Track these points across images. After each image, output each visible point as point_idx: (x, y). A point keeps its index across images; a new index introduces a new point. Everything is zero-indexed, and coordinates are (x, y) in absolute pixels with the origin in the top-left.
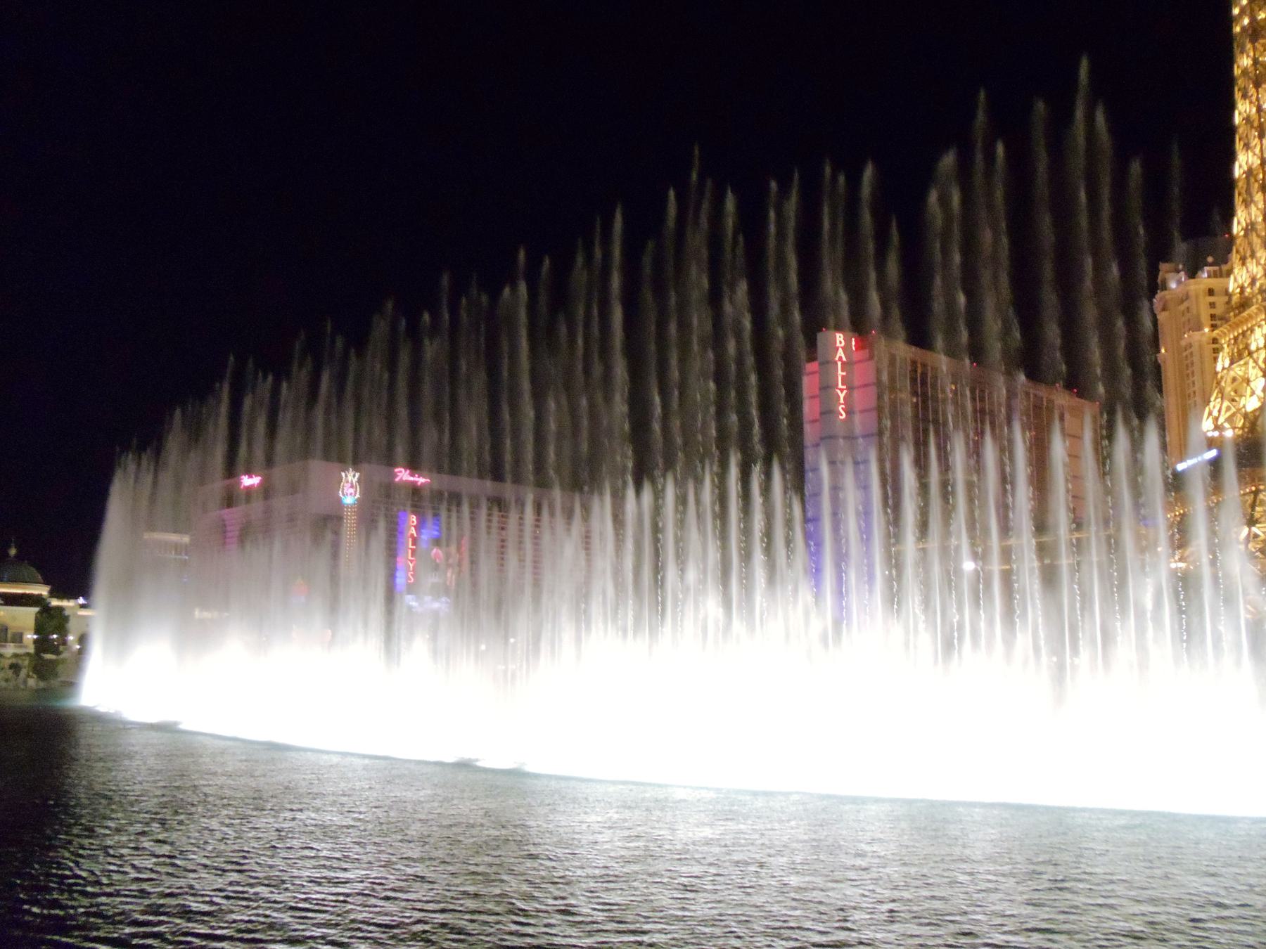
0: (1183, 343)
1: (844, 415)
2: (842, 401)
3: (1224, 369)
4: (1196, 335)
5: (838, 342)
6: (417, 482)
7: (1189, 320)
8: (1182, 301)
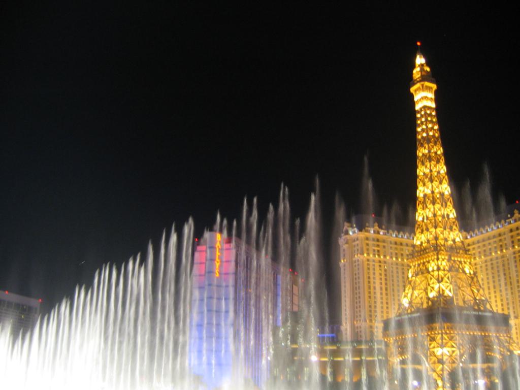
0: (354, 259)
1: (217, 275)
2: (217, 267)
8: (354, 241)
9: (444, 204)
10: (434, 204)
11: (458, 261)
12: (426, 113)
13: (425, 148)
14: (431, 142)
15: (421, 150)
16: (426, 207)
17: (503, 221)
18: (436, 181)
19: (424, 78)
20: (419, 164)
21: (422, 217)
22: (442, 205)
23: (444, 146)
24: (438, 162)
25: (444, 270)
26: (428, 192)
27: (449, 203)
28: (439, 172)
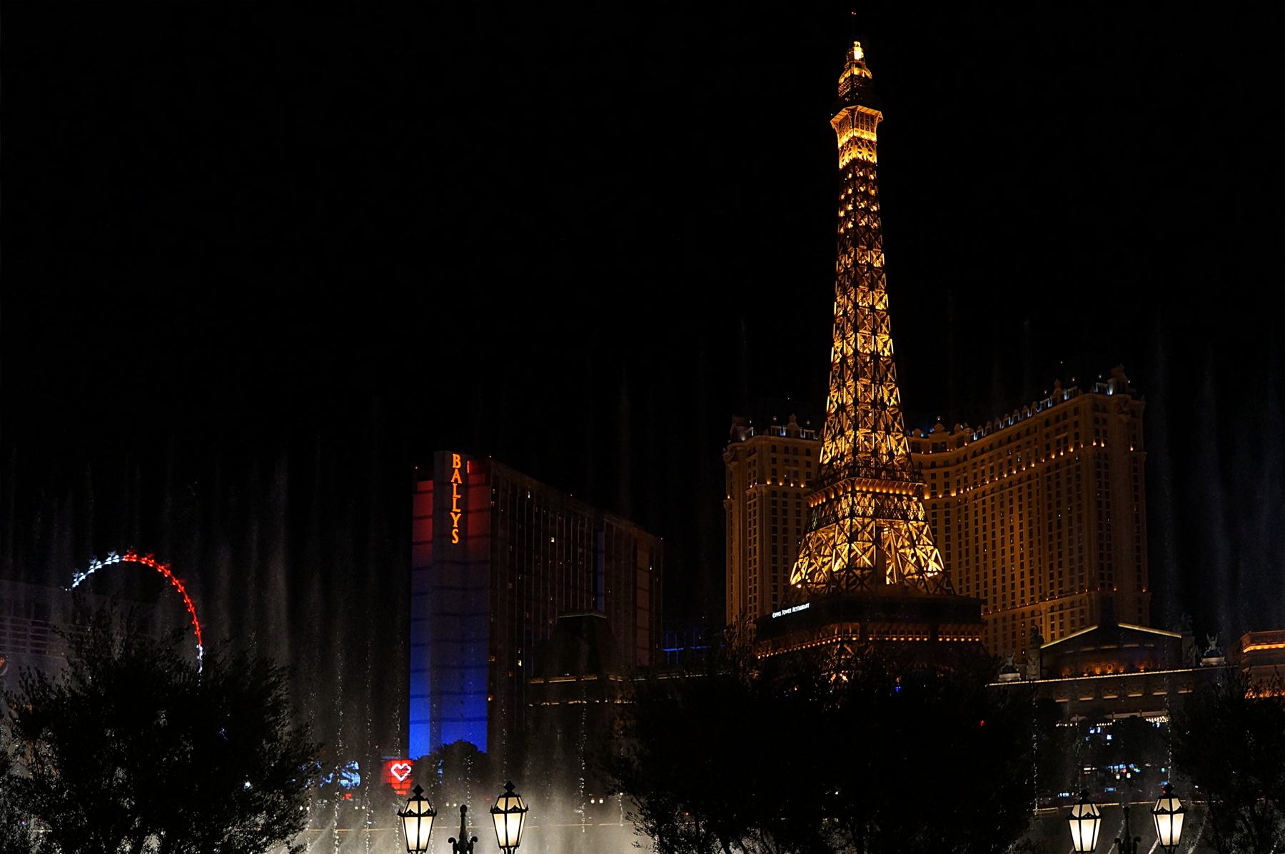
2: (455, 525)
5: (454, 463)
11: (894, 494)
13: (849, 257)
15: (843, 262)
16: (844, 385)
20: (838, 291)
22: (873, 381)
24: (872, 287)
25: (864, 515)
28: (872, 308)
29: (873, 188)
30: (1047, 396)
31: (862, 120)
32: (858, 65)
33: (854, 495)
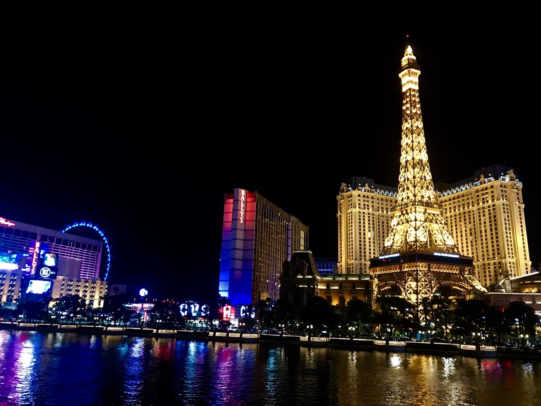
0: (348, 211)
1: (242, 222)
2: (242, 216)
3: (394, 226)
4: (354, 210)
6: (8, 225)
7: (351, 204)
8: (349, 197)
9: (422, 168)
10: (414, 168)
12: (410, 94)
14: (414, 118)
16: (408, 171)
17: (471, 184)
18: (417, 150)
19: (410, 65)
20: (404, 136)
21: (404, 178)
22: (421, 169)
23: (424, 121)
24: (419, 135)
26: (409, 158)
27: (426, 168)
28: (419, 143)
29: (417, 99)
30: (477, 181)
31: (413, 74)
32: (410, 55)
33: (415, 212)
